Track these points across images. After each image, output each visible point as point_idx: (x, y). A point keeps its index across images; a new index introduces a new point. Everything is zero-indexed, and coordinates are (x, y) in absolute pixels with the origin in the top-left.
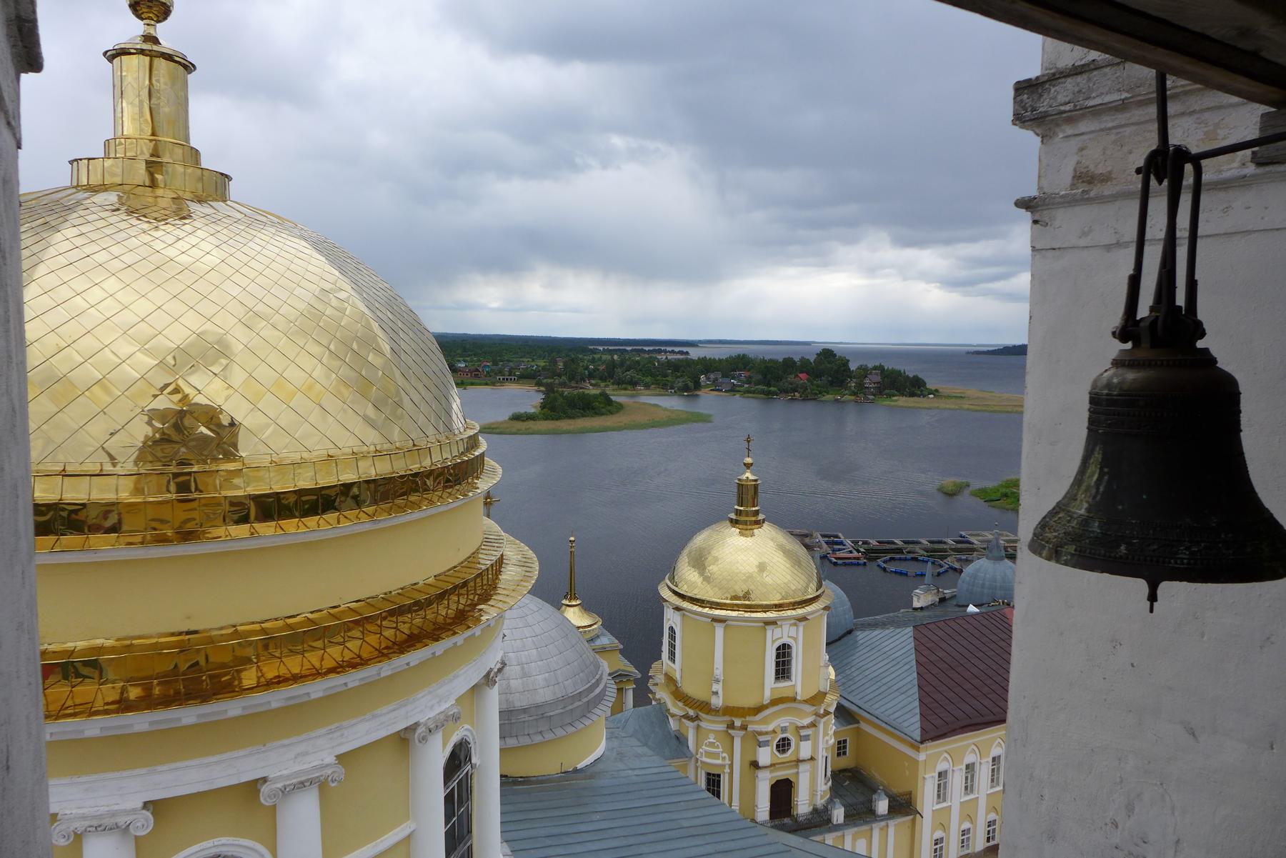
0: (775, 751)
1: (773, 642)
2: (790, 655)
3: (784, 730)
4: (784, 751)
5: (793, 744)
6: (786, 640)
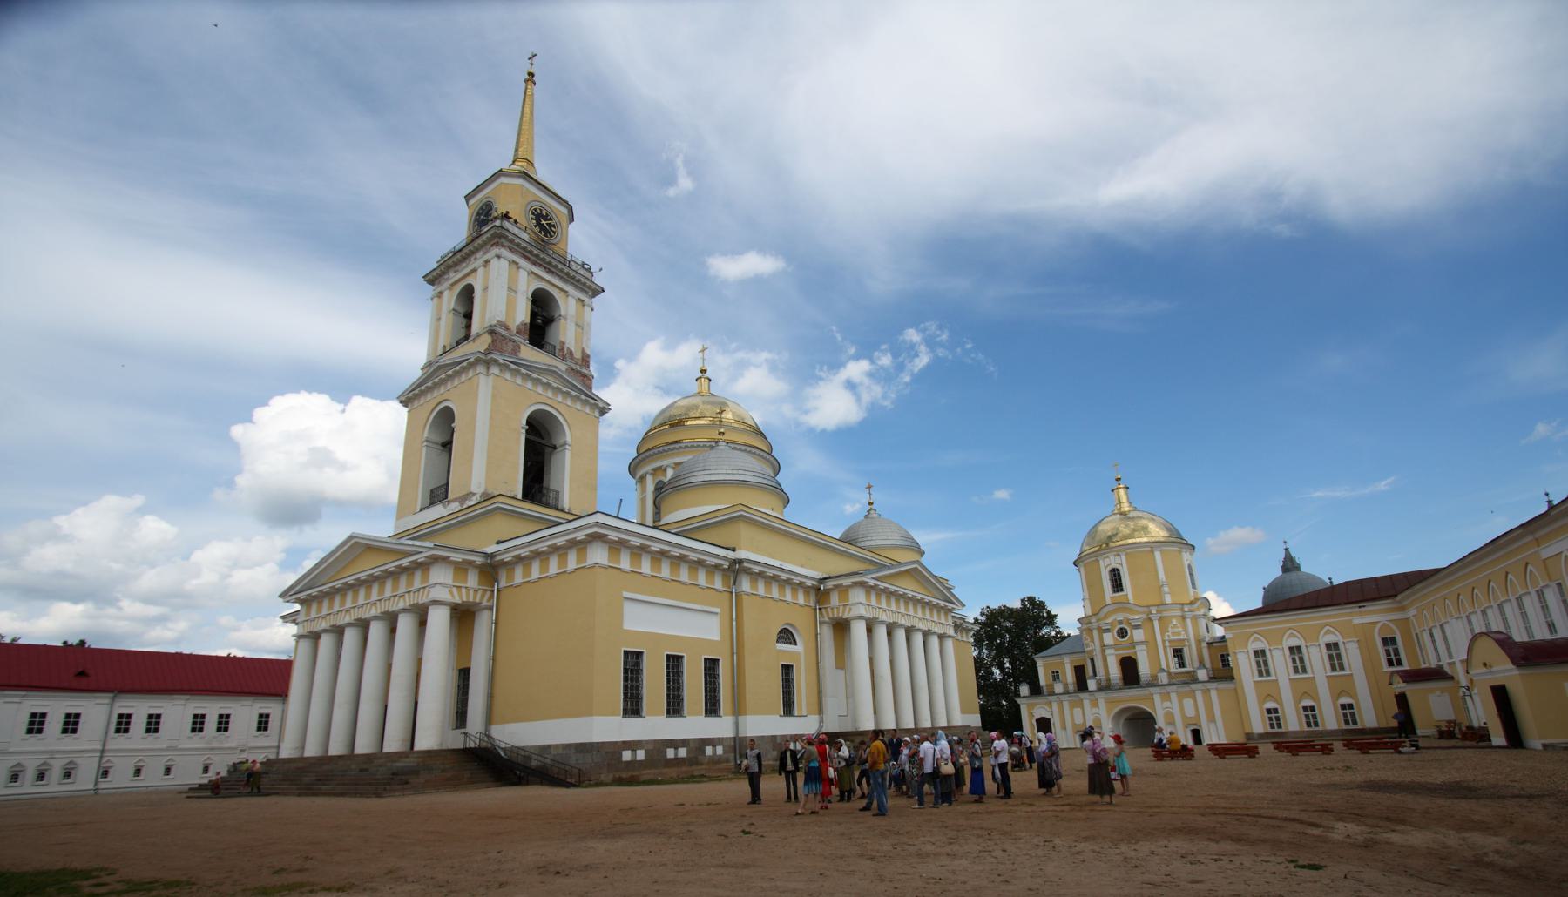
0: (1116, 636)
1: (1106, 568)
2: (1119, 574)
3: (1120, 622)
4: (1123, 637)
5: (1129, 632)
6: (1114, 566)
